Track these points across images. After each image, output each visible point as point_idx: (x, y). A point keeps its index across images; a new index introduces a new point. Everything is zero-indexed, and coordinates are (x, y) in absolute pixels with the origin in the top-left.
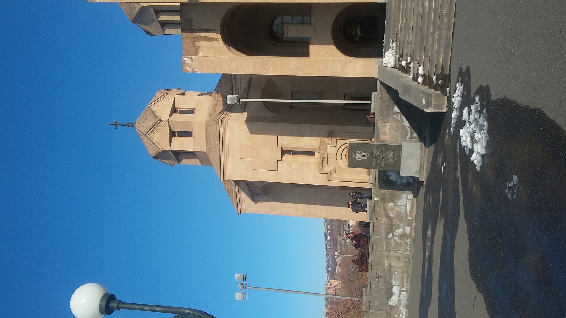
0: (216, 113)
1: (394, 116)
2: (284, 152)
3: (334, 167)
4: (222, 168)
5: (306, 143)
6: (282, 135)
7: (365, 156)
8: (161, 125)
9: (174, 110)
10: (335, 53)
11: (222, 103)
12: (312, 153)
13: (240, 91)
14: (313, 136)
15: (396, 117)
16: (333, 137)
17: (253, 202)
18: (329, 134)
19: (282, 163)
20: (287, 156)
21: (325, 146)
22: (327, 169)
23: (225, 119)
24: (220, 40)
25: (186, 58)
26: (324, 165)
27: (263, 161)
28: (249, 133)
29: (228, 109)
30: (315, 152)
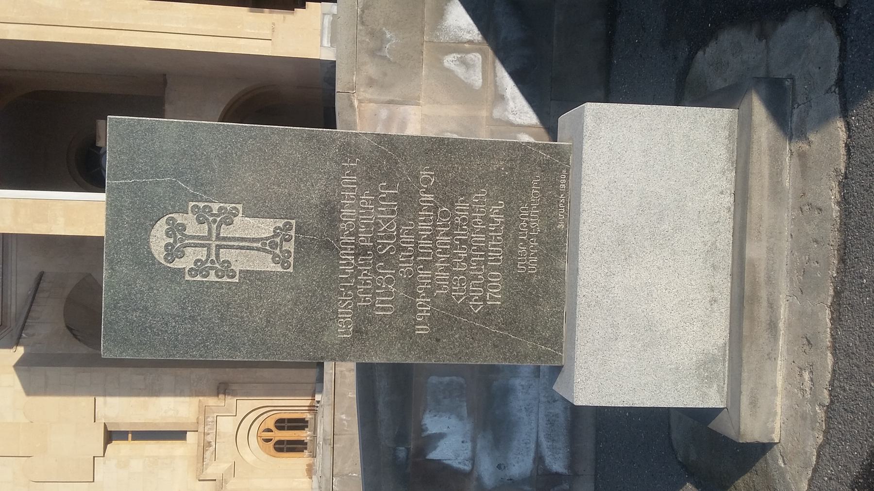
1: (450, 61)
2: (111, 436)
3: (231, 464)
6: (105, 394)
7: (268, 245)
12: (179, 435)
13: (13, 301)
14: (181, 394)
15: (460, 71)
16: (229, 394)
19: (104, 463)
21: (209, 417)
22: (214, 470)
26: (207, 461)
27: (56, 461)
28: (23, 394)
30: (185, 432)
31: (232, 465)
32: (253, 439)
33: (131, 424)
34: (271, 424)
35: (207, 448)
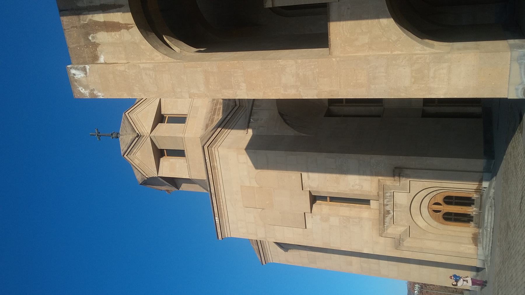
0: (213, 125)
2: (314, 199)
4: (217, 221)
5: (353, 186)
6: (308, 171)
8: (141, 143)
9: (160, 118)
10: (394, 38)
11: (222, 108)
14: (364, 173)
16: (403, 176)
17: (281, 249)
18: (394, 171)
19: (312, 217)
20: (320, 204)
21: (387, 193)
22: (394, 230)
23: (214, 146)
24: (132, 27)
25: (76, 69)
27: (280, 213)
28: (254, 168)
29: (223, 125)
30: (370, 200)
31: (406, 229)
32: (425, 210)
33: (328, 193)
34: (440, 200)
35: (387, 215)
